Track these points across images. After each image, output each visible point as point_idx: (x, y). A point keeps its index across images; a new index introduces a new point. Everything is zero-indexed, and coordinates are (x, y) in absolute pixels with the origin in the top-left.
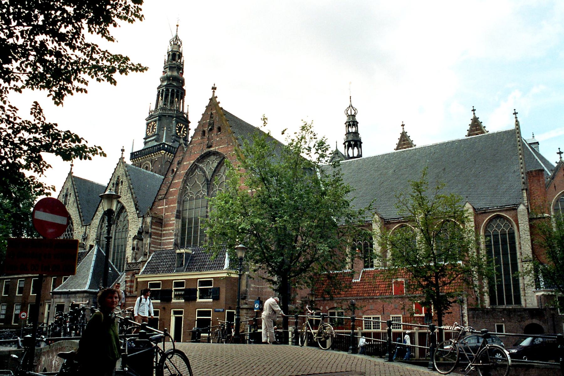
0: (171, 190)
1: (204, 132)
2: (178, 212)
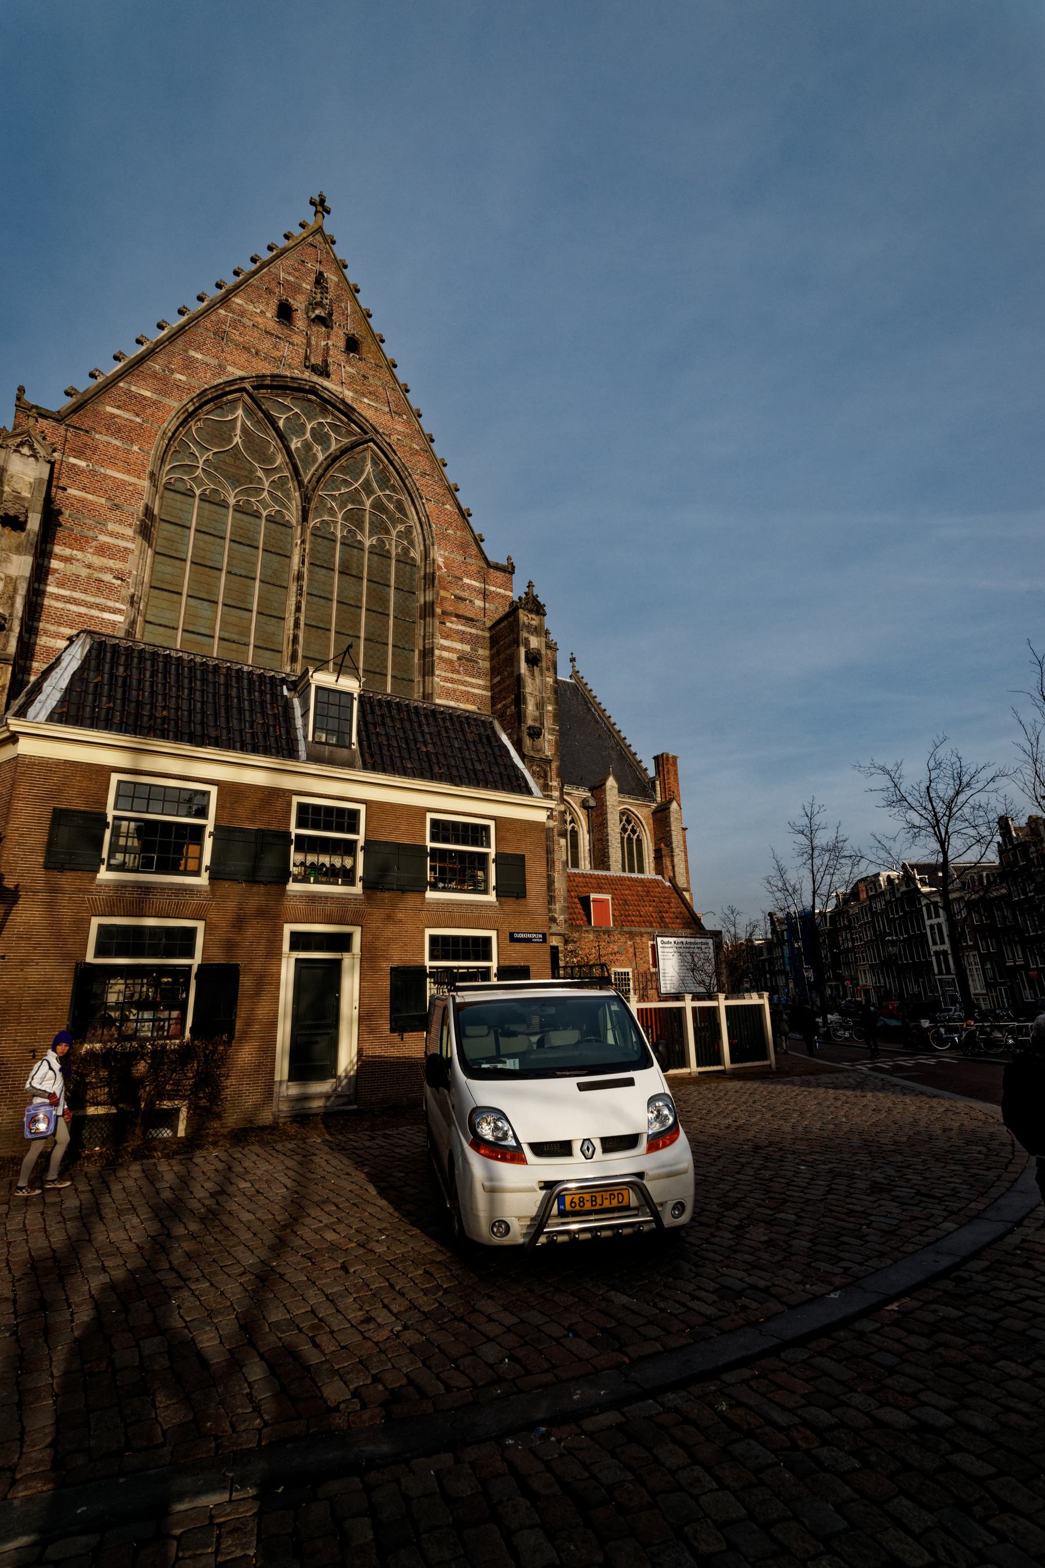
0: (109, 409)
1: (285, 313)
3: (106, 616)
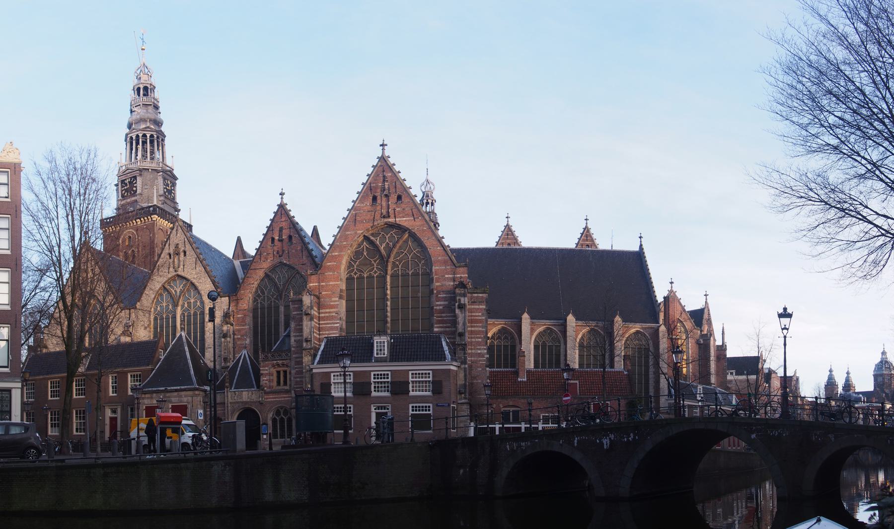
2: (341, 291)
3: (335, 325)
